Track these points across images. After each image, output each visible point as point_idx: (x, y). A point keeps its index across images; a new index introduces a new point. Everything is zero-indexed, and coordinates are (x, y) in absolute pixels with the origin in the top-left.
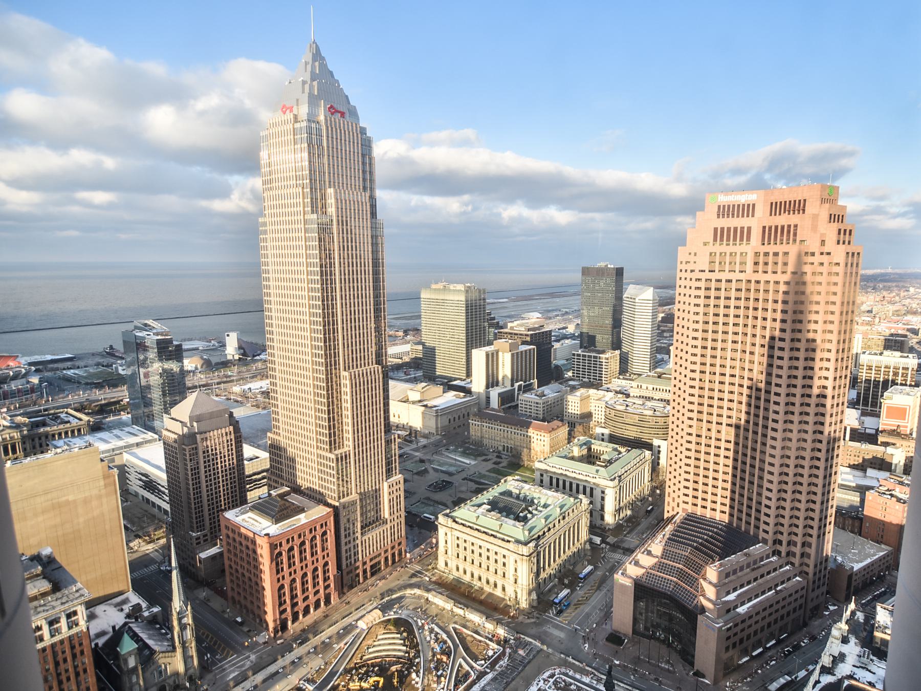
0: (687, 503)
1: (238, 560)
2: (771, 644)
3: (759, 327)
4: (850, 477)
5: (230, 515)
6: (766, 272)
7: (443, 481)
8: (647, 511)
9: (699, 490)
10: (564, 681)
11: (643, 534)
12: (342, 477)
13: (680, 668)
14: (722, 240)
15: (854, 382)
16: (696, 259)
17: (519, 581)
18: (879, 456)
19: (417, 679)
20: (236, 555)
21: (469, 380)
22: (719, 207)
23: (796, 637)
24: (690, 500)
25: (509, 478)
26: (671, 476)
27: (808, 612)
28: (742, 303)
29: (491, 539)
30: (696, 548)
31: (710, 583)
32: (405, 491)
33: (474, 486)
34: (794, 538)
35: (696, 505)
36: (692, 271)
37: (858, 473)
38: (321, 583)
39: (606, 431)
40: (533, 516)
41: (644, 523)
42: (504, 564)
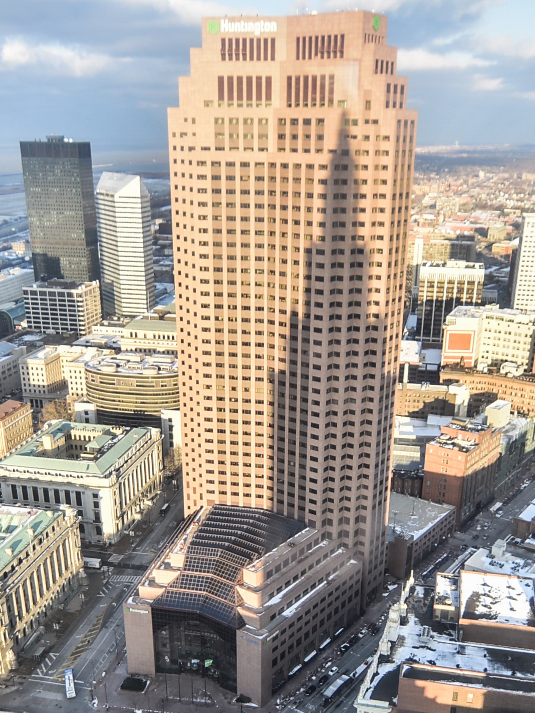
0: (213, 492)
2: (325, 643)
3: (289, 235)
4: (410, 429)
6: (295, 150)
8: (162, 511)
9: (228, 469)
11: (158, 543)
13: (220, 699)
14: (231, 98)
15: (413, 304)
16: (195, 128)
18: (441, 398)
22: (223, 40)
23: (353, 630)
24: (216, 487)
26: (189, 460)
27: (366, 598)
28: (265, 199)
30: (228, 549)
31: (249, 588)
34: (346, 514)
35: (224, 493)
36: (191, 149)
37: (418, 422)
39: (91, 407)
41: (159, 527)
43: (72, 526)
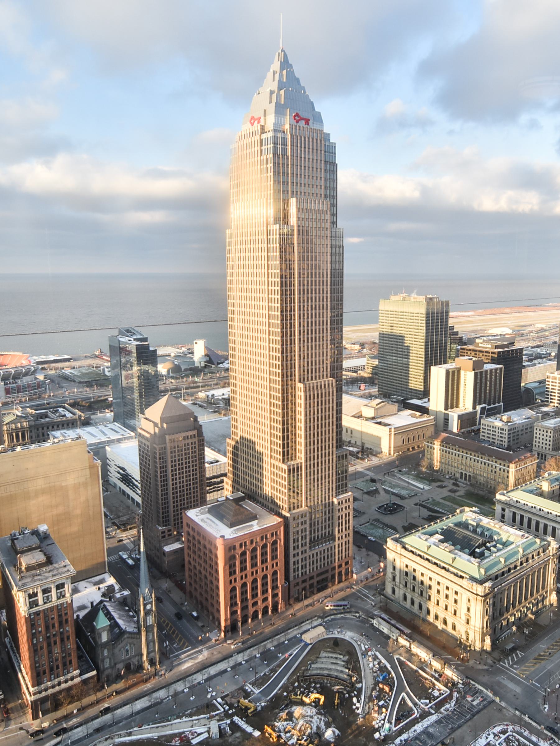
1: (196, 557)
5: (192, 514)
7: (394, 504)
10: (518, 740)
12: (293, 489)
17: (472, 622)
19: (358, 705)
20: (194, 552)
21: (426, 400)
25: (467, 509)
29: (443, 572)
32: (354, 510)
33: (426, 513)
38: (270, 591)
40: (492, 553)
42: (456, 601)
43: (553, 555)
